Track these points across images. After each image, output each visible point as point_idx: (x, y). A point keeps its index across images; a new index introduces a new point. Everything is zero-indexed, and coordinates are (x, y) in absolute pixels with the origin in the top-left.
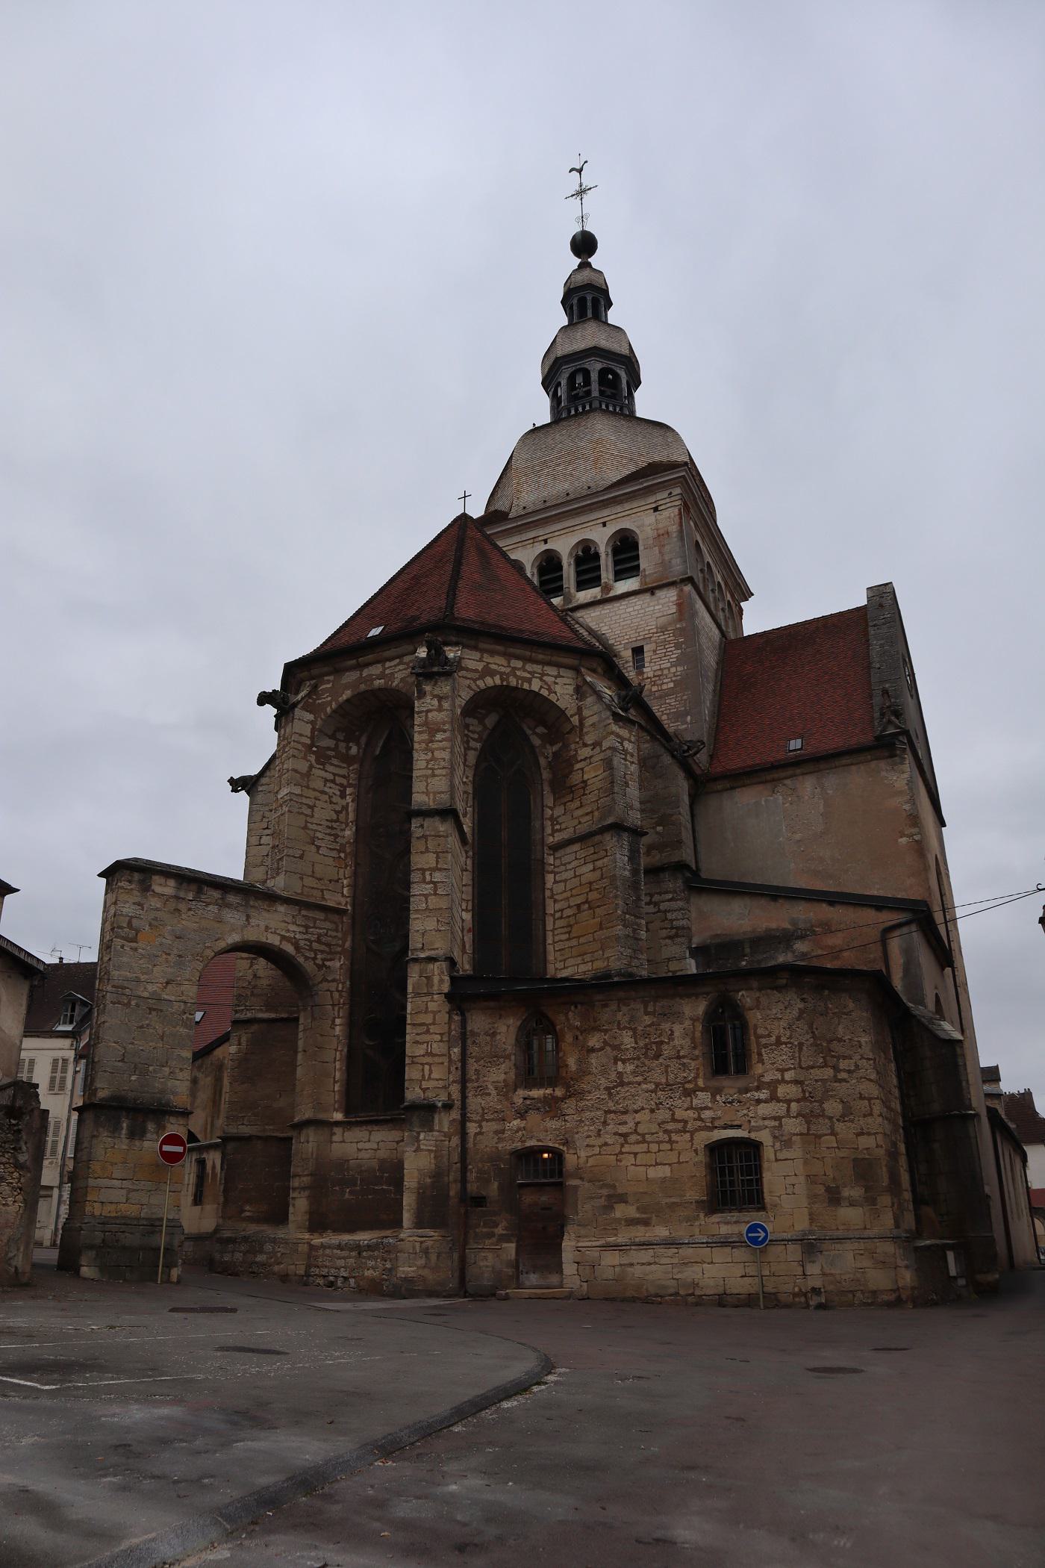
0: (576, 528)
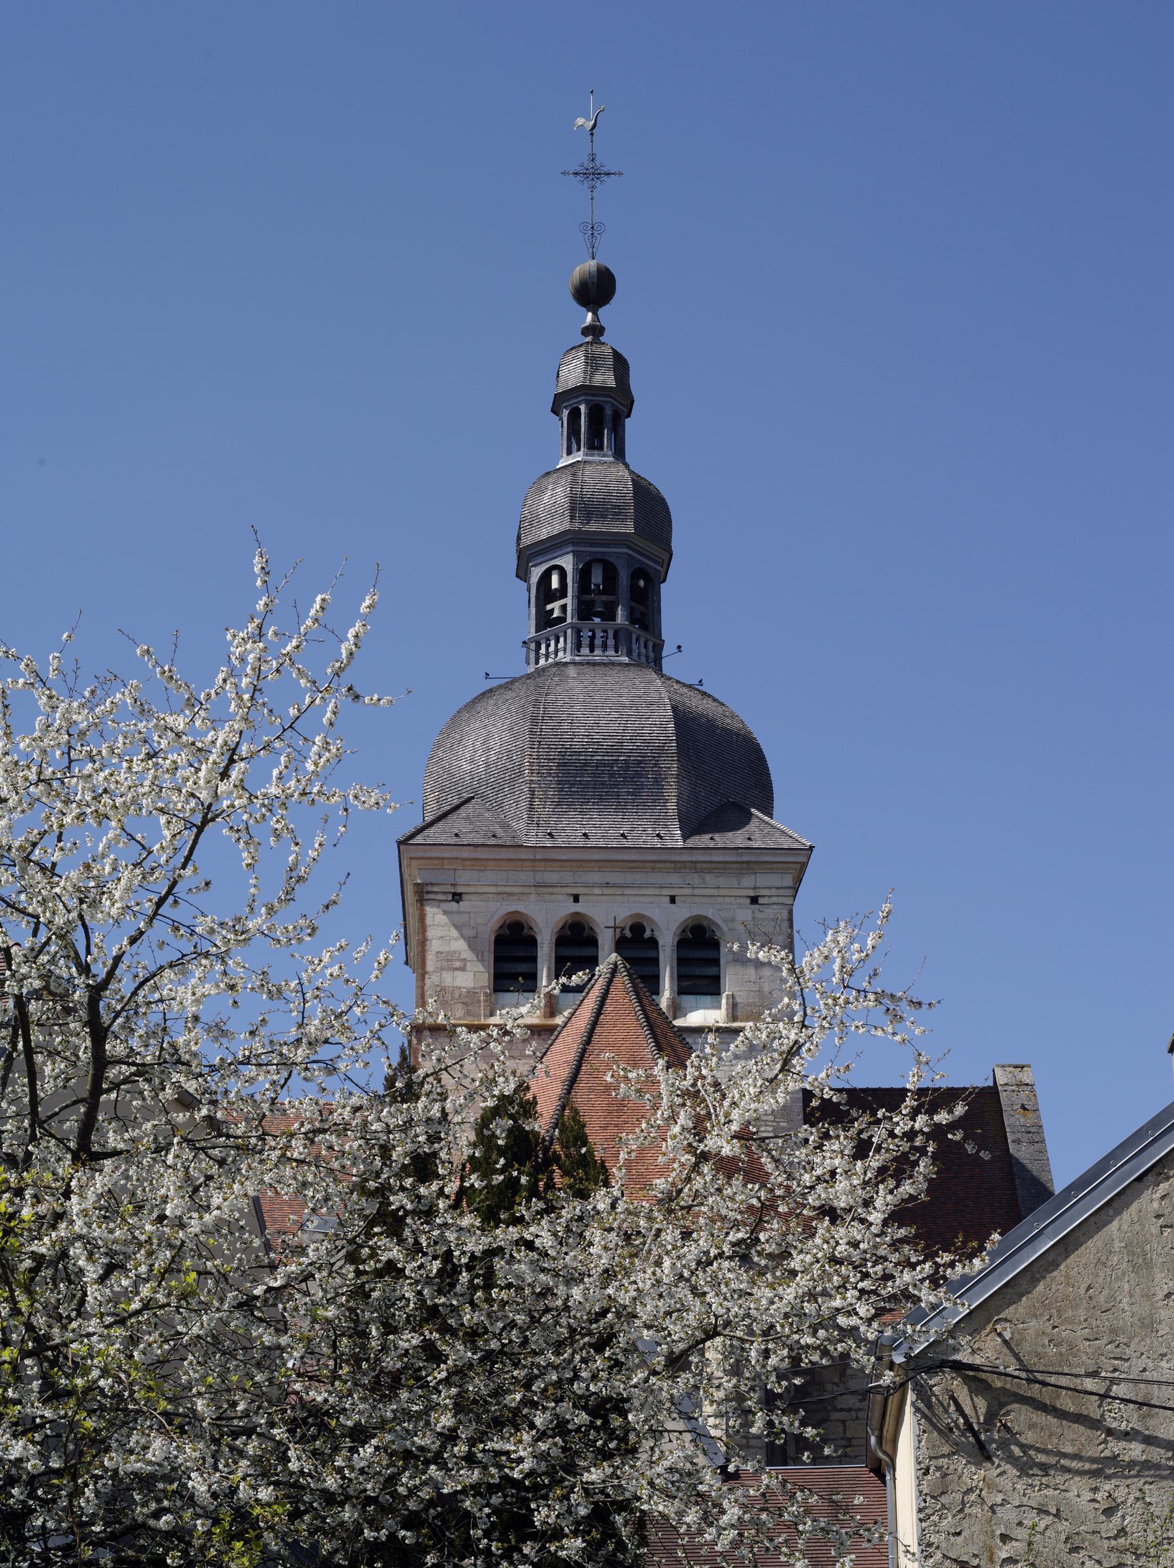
0: (627, 891)
